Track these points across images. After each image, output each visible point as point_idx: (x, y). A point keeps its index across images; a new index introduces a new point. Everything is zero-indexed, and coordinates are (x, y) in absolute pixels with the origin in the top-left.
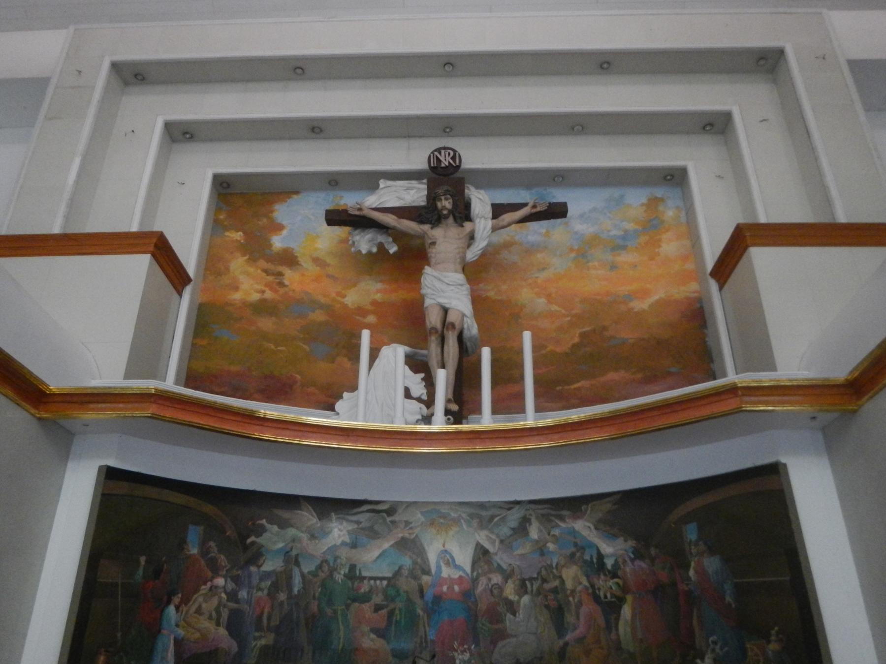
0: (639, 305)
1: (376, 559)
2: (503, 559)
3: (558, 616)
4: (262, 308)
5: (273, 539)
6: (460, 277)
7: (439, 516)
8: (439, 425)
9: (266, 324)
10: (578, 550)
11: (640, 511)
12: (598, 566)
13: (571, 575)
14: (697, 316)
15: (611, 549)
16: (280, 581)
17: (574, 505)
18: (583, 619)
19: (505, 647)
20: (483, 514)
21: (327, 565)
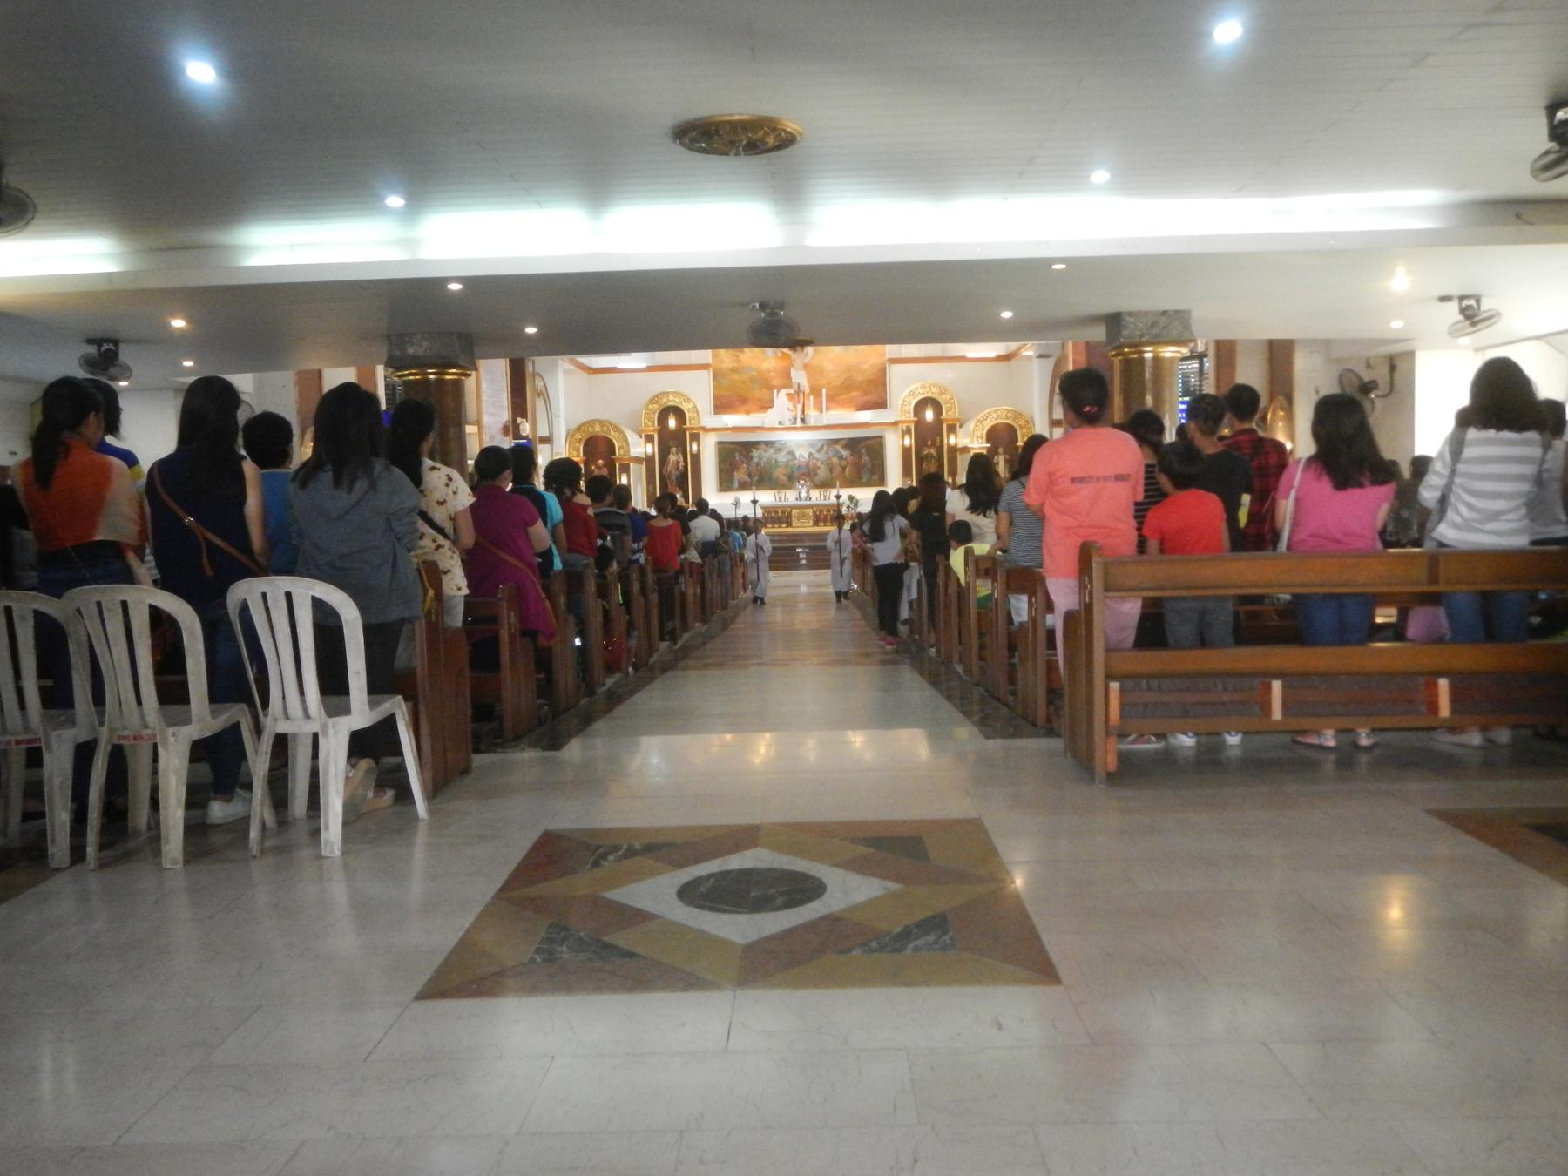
0: (866, 366)
1: (782, 457)
2: (816, 455)
3: (831, 470)
4: (734, 370)
5: (755, 453)
6: (803, 373)
7: (799, 445)
8: (799, 424)
9: (736, 376)
10: (837, 453)
11: (852, 444)
12: (841, 458)
13: (835, 460)
14: (883, 371)
15: (845, 453)
16: (758, 464)
17: (836, 441)
18: (837, 470)
19: (817, 479)
20: (812, 444)
21: (769, 460)
